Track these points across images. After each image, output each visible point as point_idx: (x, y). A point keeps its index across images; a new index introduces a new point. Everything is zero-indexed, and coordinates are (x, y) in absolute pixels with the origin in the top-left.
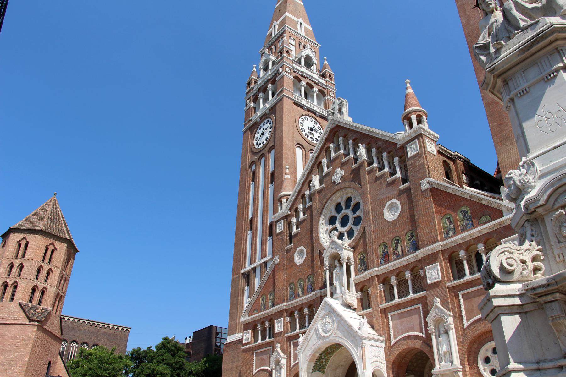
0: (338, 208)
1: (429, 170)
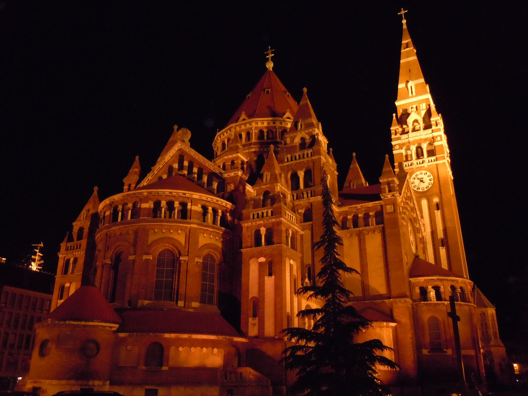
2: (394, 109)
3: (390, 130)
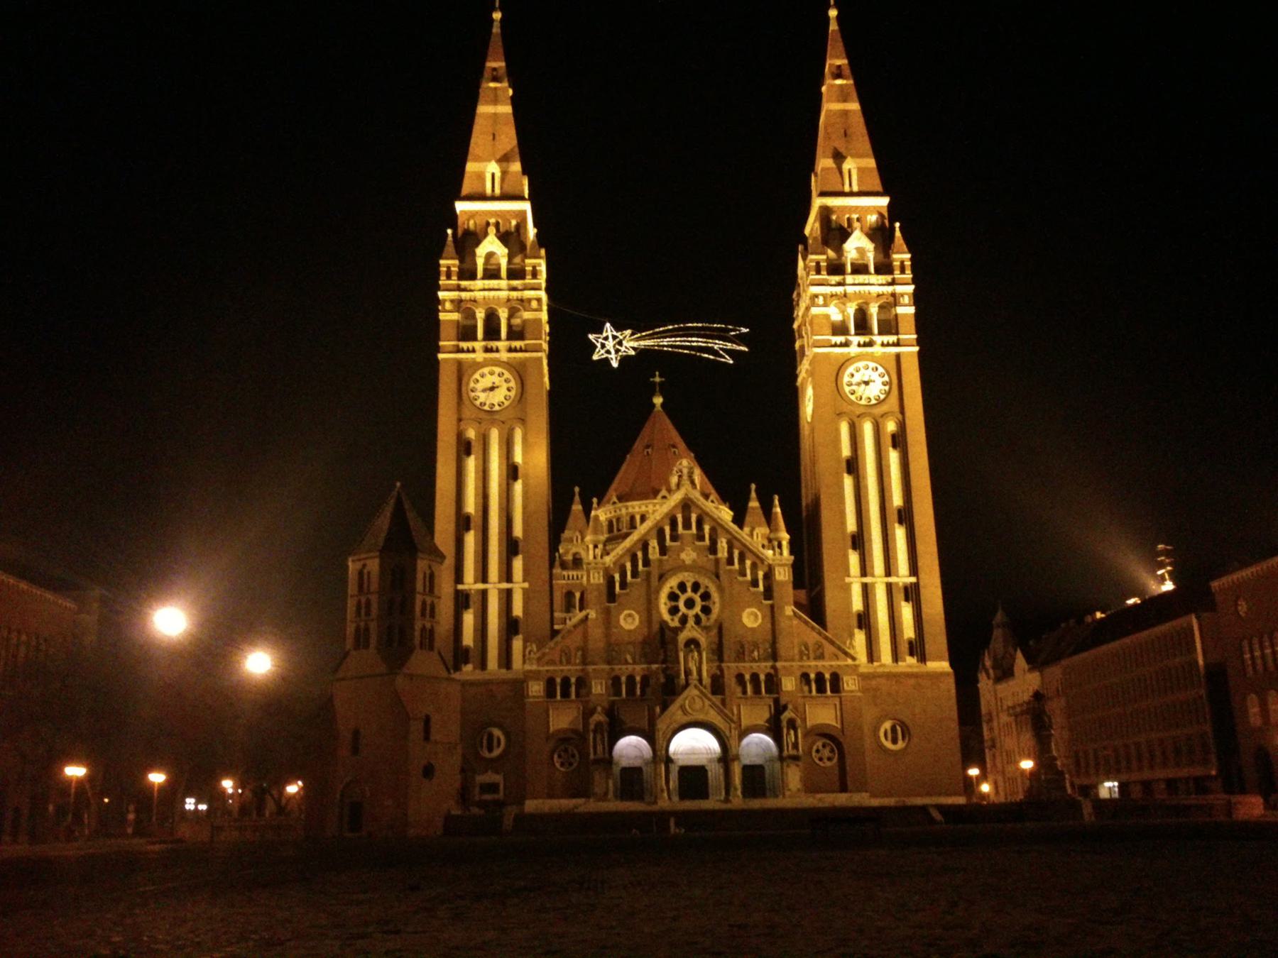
0: (682, 587)
2: (452, 218)
3: (439, 265)
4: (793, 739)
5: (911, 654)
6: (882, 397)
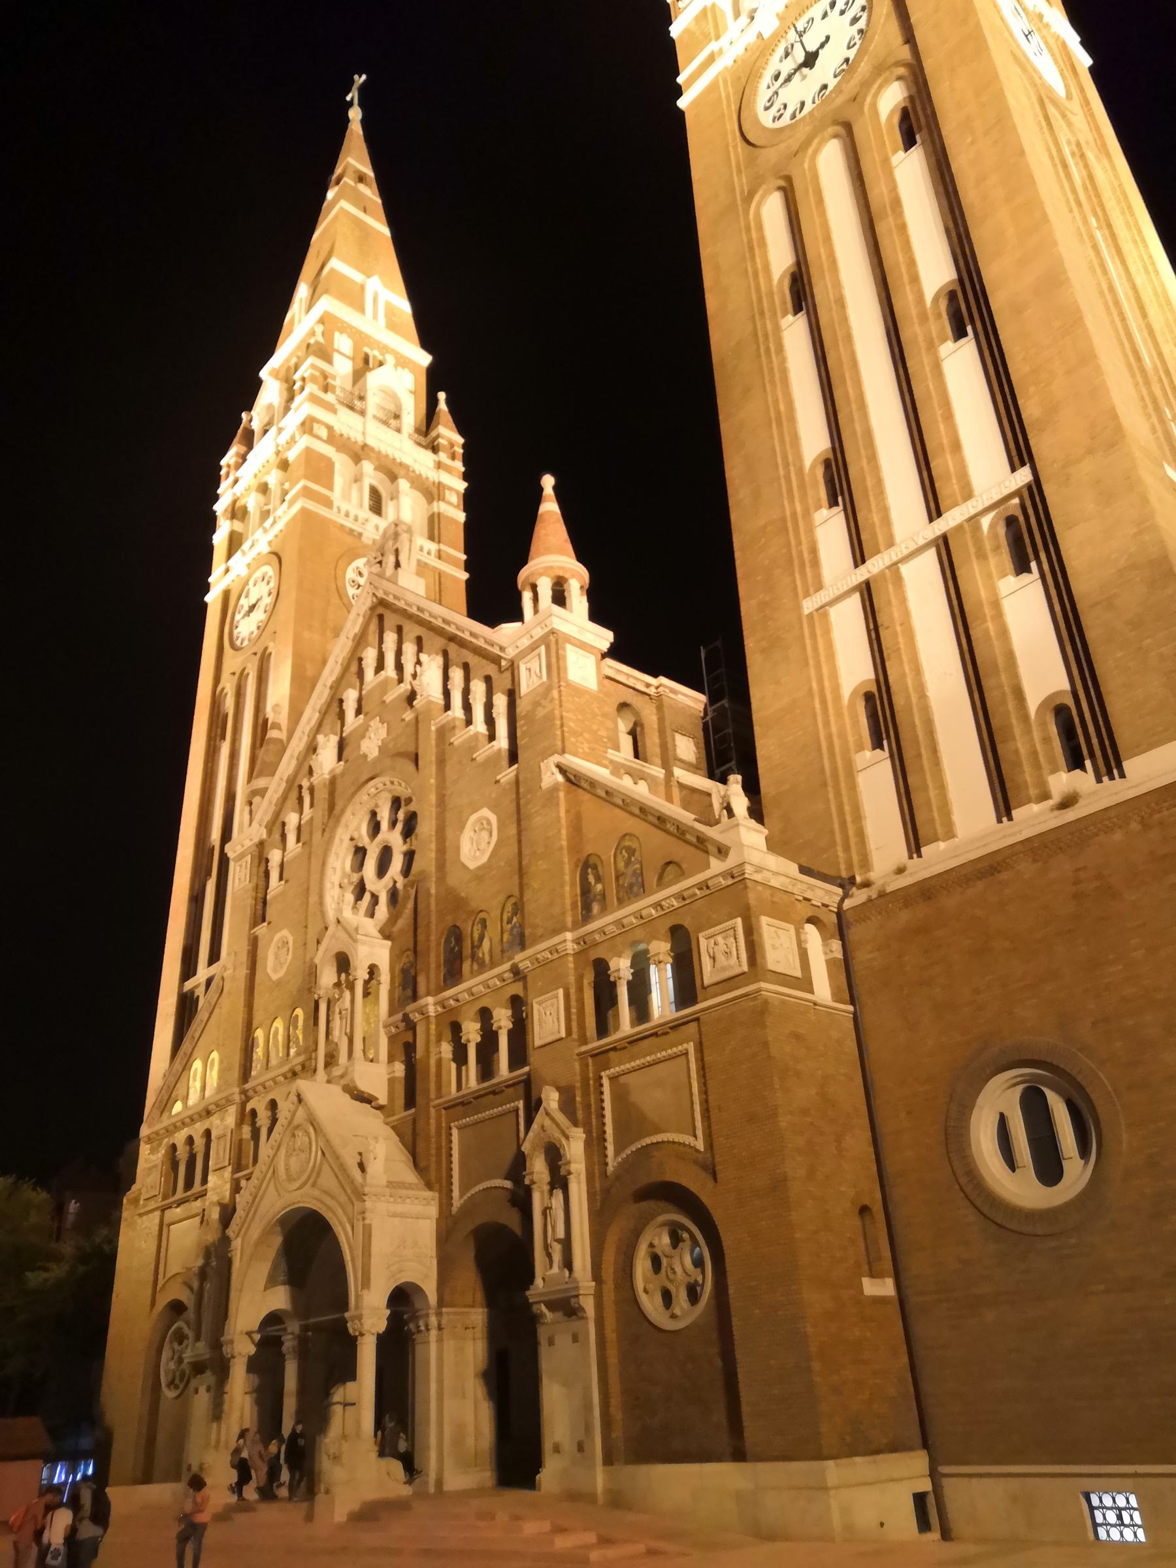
0: (375, 828)
1: (563, 732)
4: (561, 1234)
5: (1075, 762)
6: (851, 54)
